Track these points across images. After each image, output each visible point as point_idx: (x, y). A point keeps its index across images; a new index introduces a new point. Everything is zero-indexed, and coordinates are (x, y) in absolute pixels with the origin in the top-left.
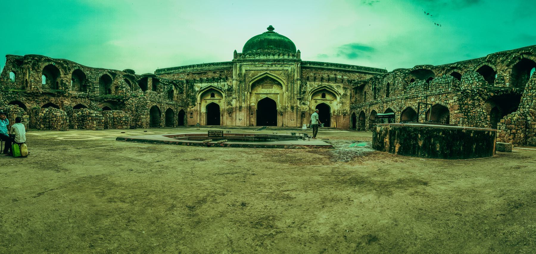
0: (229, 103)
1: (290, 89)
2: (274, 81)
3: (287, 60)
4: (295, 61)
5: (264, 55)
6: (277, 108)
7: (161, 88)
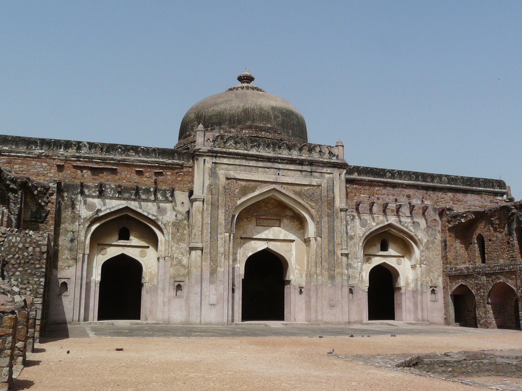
1: (325, 230)
4: (335, 165)
5: (268, 146)
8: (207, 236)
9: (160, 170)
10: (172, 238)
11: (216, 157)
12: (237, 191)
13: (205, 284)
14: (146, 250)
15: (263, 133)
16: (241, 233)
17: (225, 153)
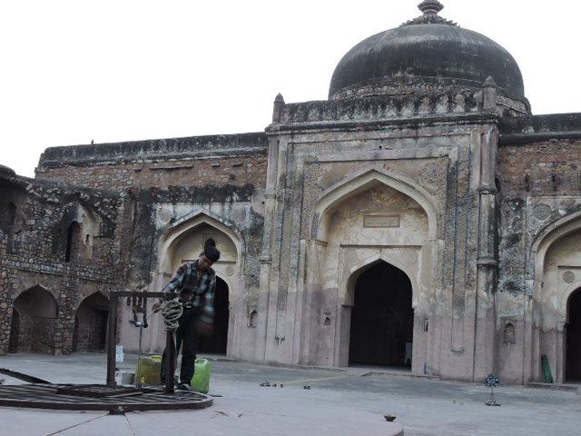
0: (253, 281)
2: (406, 197)
3: (443, 120)
4: (472, 120)
5: (367, 107)
6: (415, 304)
7: (31, 215)
8: (277, 246)
9: (239, 161)
10: (249, 251)
11: (292, 135)
12: (319, 179)
13: (273, 309)
14: (233, 266)
15: (385, 88)
16: (341, 238)
17: (304, 128)
